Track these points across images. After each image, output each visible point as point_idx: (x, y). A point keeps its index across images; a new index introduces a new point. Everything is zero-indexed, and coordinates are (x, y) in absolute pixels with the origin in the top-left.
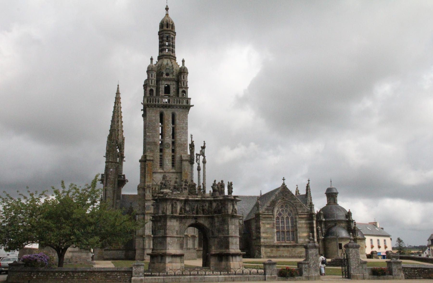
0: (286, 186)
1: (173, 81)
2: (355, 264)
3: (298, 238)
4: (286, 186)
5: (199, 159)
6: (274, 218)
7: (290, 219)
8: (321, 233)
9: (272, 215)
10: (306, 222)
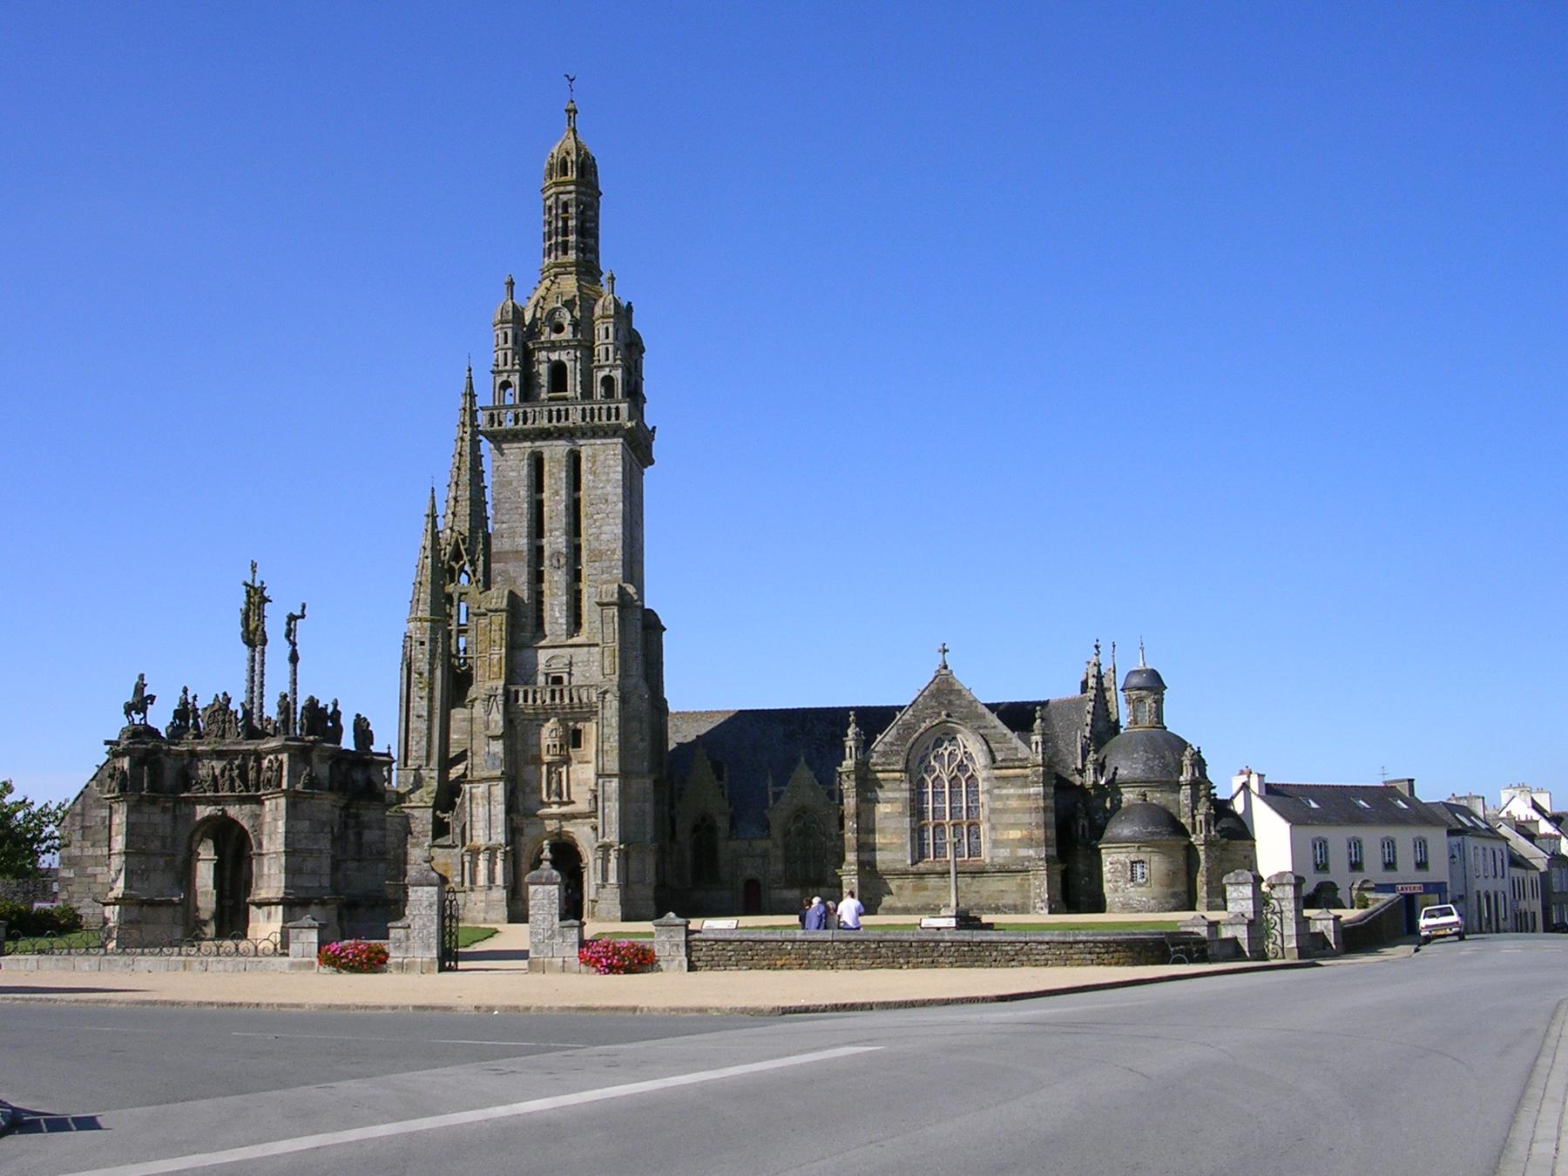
1: (575, 348)
2: (541, 931)
4: (951, 672)
5: (295, 630)
9: (900, 771)
10: (1020, 791)
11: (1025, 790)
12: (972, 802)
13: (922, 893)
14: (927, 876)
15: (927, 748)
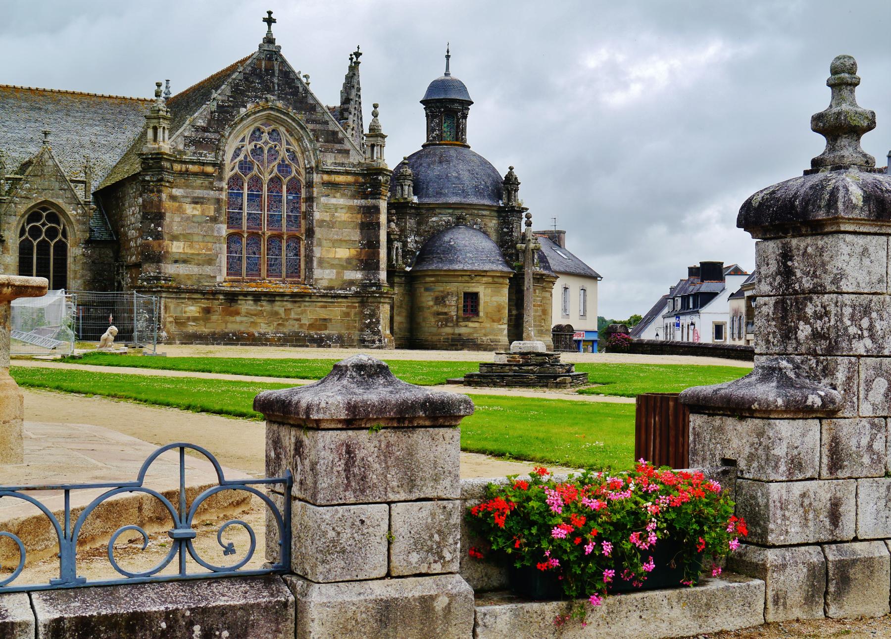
0: (280, 47)
3: (315, 264)
4: (280, 47)
6: (221, 179)
7: (285, 187)
8: (400, 251)
9: (214, 165)
11: (356, 201)
12: (292, 212)
13: (232, 319)
14: (240, 298)
15: (243, 140)
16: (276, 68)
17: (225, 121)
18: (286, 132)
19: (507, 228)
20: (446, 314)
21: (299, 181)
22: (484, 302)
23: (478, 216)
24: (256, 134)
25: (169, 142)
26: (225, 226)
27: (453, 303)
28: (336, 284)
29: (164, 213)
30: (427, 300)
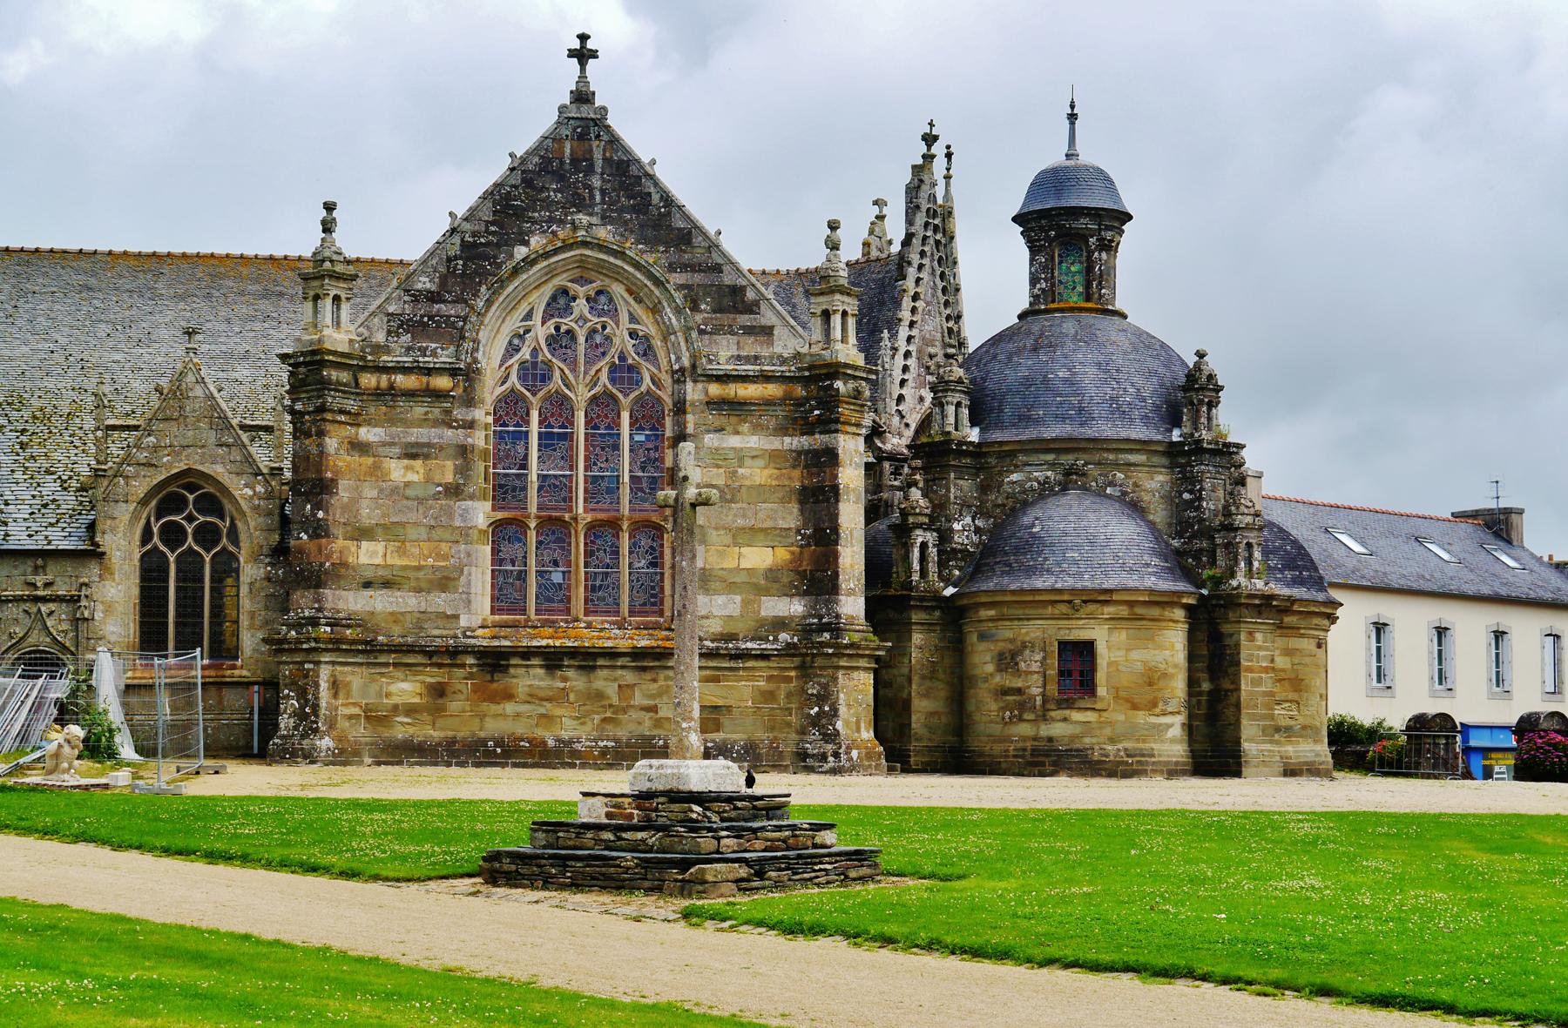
0: (604, 109)
6: (470, 401)
7: (625, 417)
8: (933, 551)
9: (453, 372)
11: (787, 440)
12: (643, 469)
14: (514, 661)
15: (529, 316)
16: (598, 156)
17: (480, 275)
18: (626, 295)
19: (1191, 492)
20: (1019, 691)
21: (659, 399)
22: (1109, 664)
23: (1116, 465)
24: (560, 302)
25: (352, 328)
26: (488, 505)
27: (1035, 667)
28: (740, 628)
29: (334, 481)
30: (983, 660)
